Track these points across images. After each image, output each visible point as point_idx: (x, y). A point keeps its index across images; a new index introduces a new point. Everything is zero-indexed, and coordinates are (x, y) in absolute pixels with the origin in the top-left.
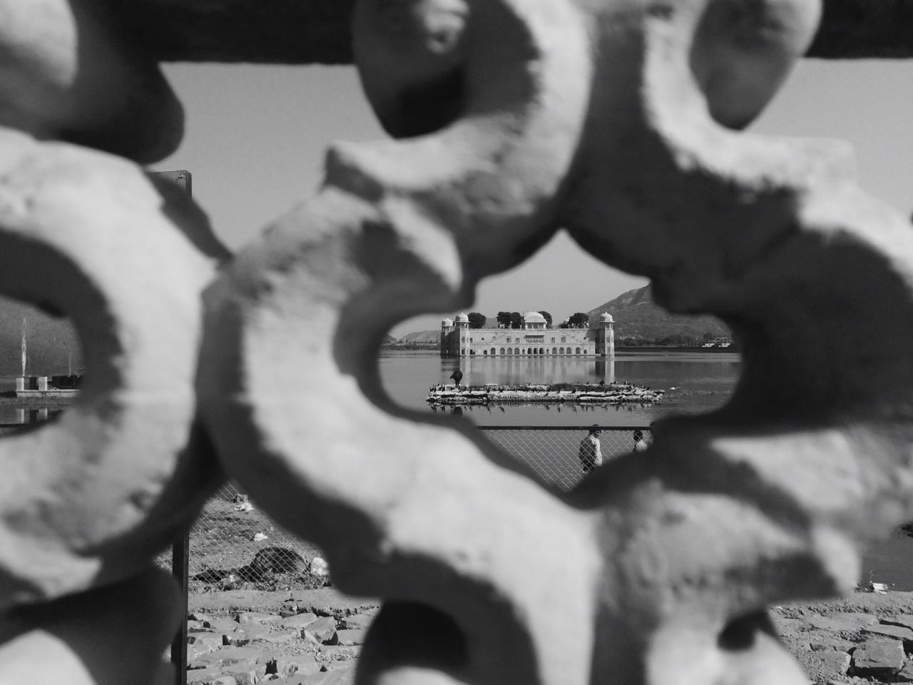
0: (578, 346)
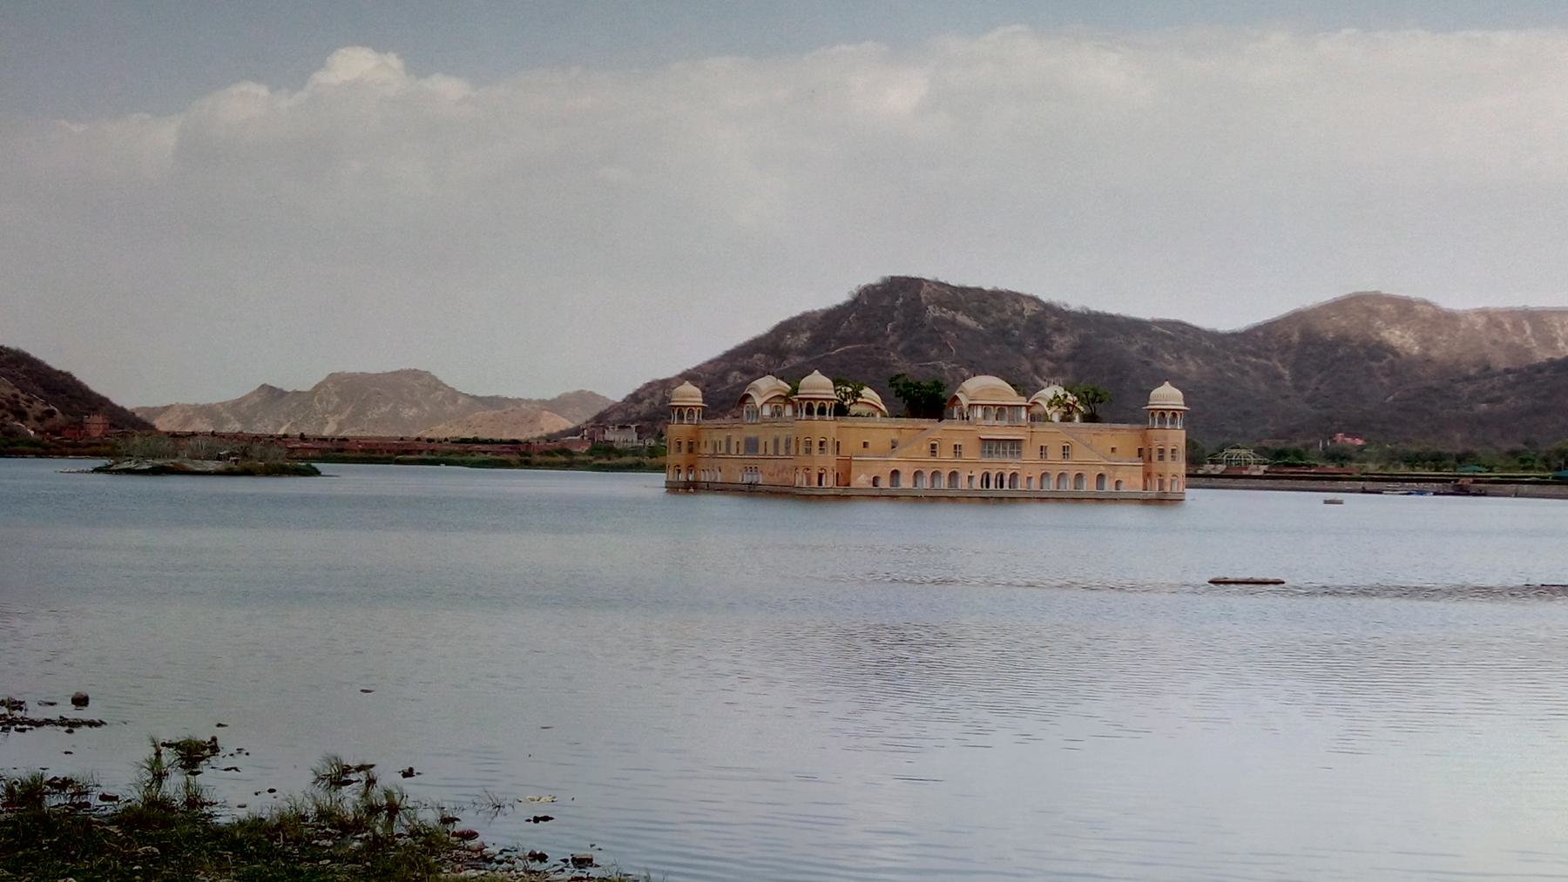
0: (1102, 470)
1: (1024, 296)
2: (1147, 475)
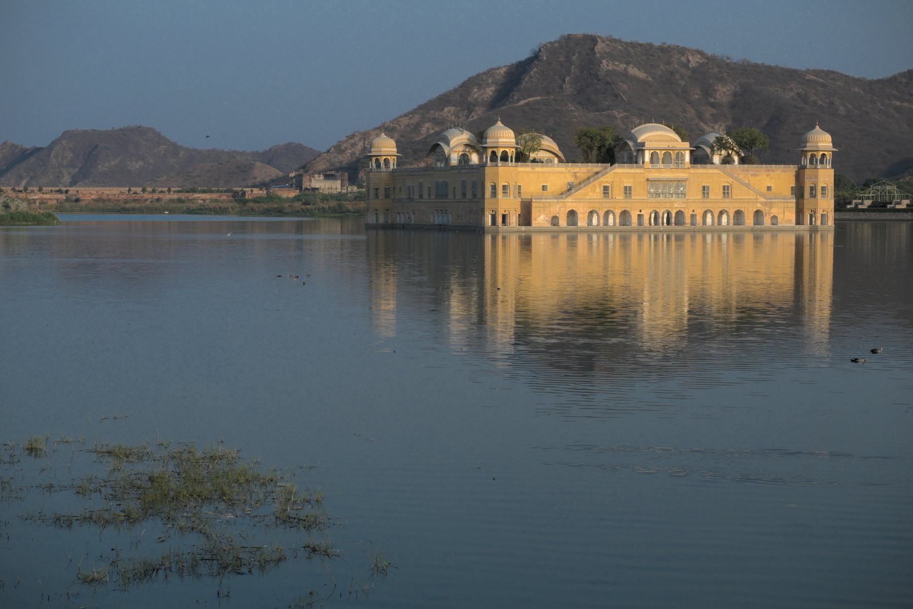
0: (759, 206)
1: (689, 50)
2: (799, 212)
